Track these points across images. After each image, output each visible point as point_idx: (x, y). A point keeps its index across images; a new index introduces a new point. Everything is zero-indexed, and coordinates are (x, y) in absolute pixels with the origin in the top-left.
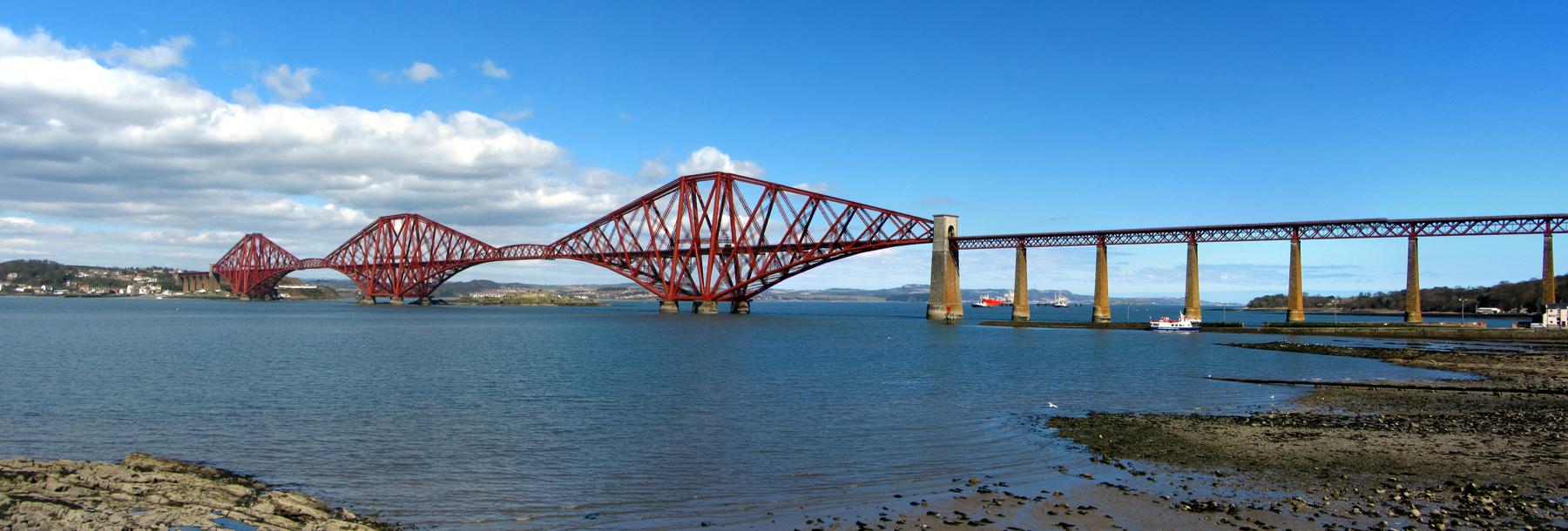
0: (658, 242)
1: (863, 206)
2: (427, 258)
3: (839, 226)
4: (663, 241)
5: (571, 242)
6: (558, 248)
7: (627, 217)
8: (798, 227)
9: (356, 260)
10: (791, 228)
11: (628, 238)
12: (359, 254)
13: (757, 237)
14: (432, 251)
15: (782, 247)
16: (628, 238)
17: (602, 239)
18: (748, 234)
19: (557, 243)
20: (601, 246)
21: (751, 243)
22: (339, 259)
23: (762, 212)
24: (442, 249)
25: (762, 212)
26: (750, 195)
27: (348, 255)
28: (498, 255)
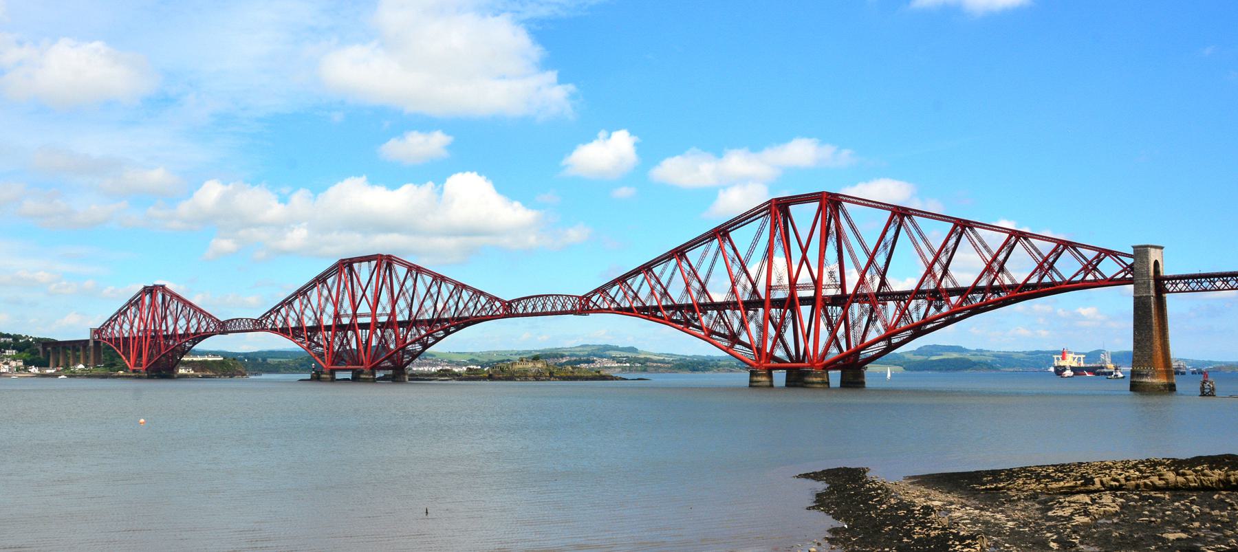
12: (126, 327)
13: (406, 313)
22: (110, 330)
27: (117, 327)
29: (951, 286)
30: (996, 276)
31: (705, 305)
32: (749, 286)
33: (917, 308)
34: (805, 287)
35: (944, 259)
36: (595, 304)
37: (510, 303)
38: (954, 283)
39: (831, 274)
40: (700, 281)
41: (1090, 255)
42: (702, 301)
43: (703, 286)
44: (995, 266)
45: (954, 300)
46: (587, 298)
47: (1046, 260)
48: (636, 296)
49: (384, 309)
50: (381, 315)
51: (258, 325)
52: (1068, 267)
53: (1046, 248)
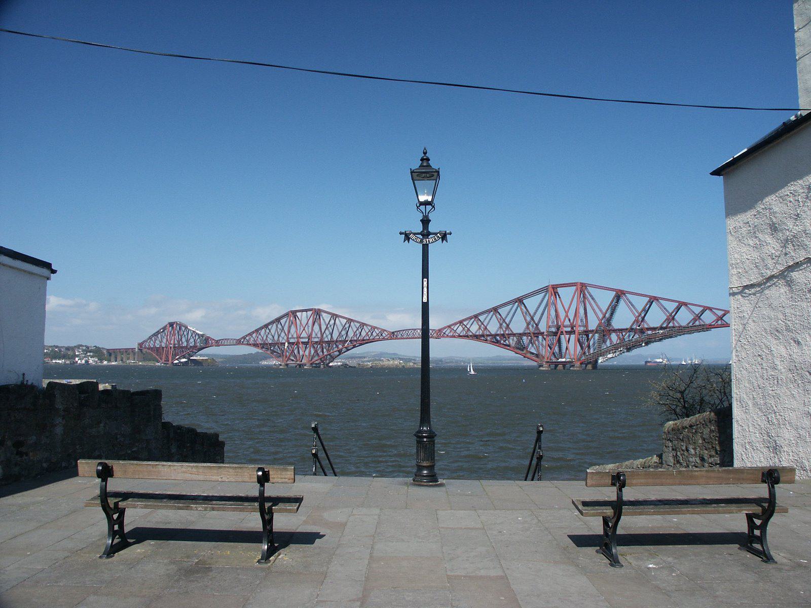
0: (281, 339)
1: (367, 325)
2: (185, 344)
3: (357, 332)
4: (283, 338)
5: (247, 338)
6: (242, 340)
7: (270, 327)
8: (344, 333)
9: (156, 345)
10: (340, 333)
11: (270, 336)
13: (329, 337)
14: (187, 341)
15: (337, 341)
16: (270, 336)
17: (260, 337)
18: (325, 335)
19: (241, 339)
20: (259, 340)
21: (326, 340)
23: (330, 326)
24: (192, 340)
25: (330, 326)
26: (326, 317)
28: (218, 343)
29: (646, 326)
30: (641, 324)
31: (508, 334)
32: (535, 325)
33: (629, 336)
34: (566, 326)
35: (643, 315)
36: (444, 333)
37: (217, 341)
38: (648, 324)
39: (582, 321)
40: (506, 323)
41: (720, 313)
42: (507, 332)
43: (508, 325)
44: (671, 318)
45: (650, 332)
46: (440, 330)
47: (697, 315)
48: (469, 329)
49: (316, 335)
50: (315, 338)
51: (239, 342)
52: (708, 318)
53: (698, 310)
